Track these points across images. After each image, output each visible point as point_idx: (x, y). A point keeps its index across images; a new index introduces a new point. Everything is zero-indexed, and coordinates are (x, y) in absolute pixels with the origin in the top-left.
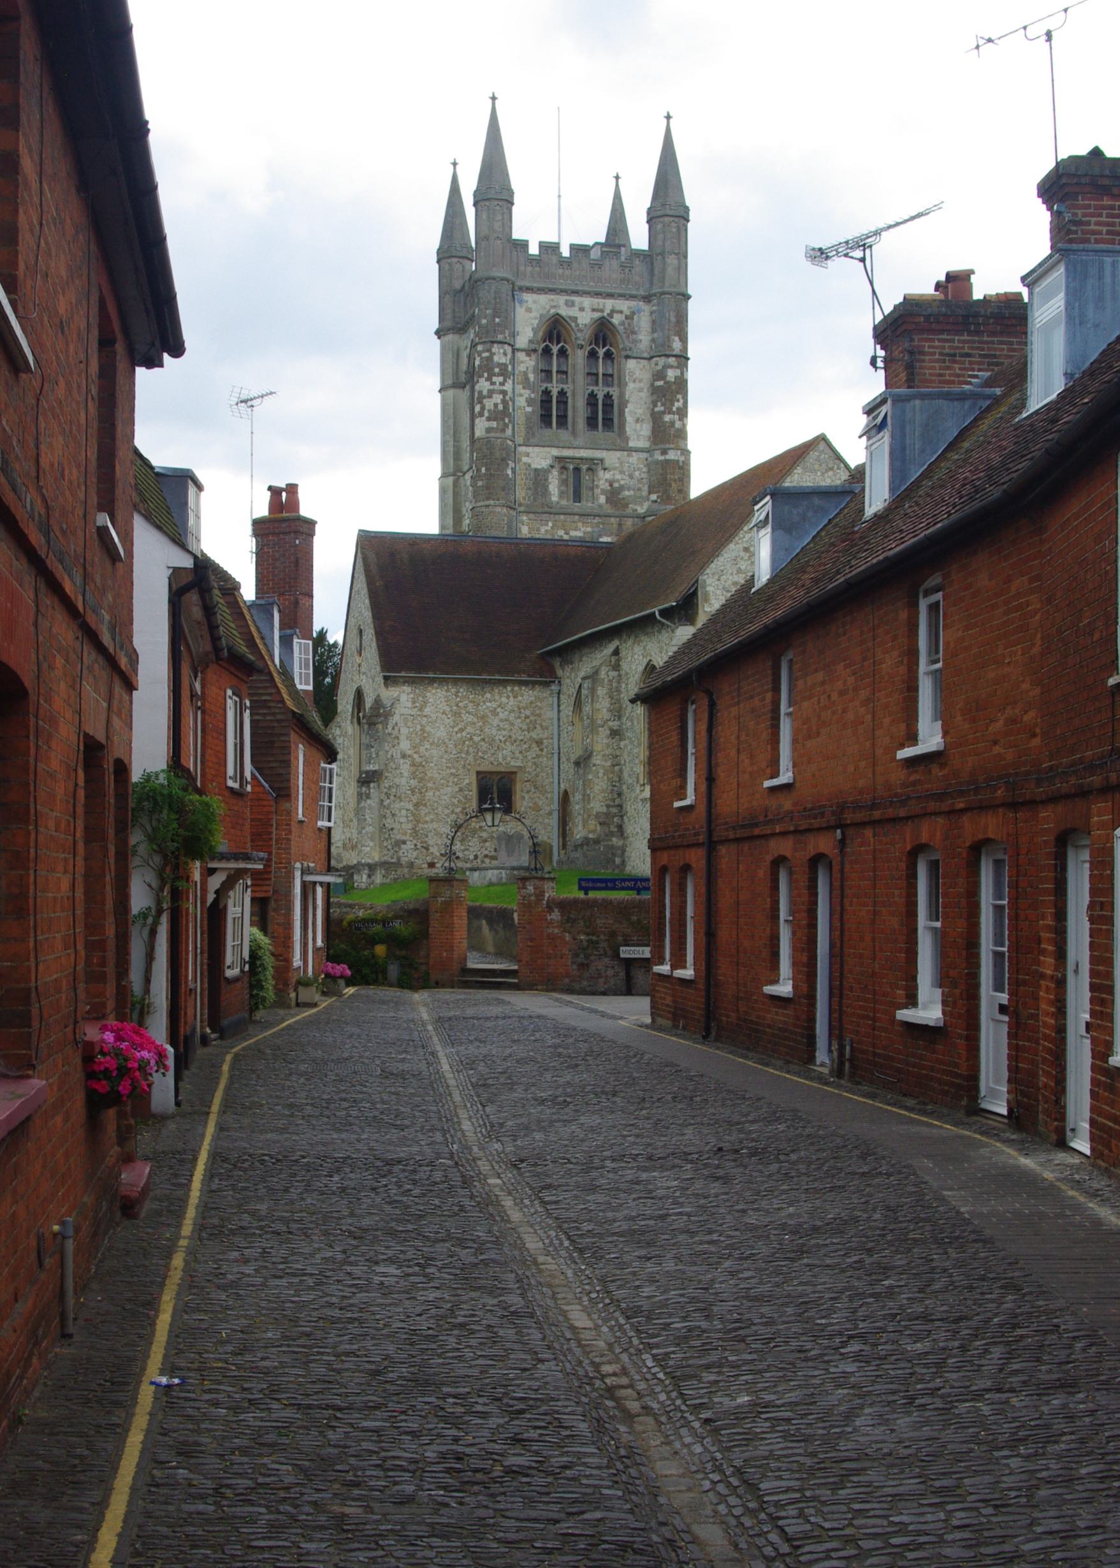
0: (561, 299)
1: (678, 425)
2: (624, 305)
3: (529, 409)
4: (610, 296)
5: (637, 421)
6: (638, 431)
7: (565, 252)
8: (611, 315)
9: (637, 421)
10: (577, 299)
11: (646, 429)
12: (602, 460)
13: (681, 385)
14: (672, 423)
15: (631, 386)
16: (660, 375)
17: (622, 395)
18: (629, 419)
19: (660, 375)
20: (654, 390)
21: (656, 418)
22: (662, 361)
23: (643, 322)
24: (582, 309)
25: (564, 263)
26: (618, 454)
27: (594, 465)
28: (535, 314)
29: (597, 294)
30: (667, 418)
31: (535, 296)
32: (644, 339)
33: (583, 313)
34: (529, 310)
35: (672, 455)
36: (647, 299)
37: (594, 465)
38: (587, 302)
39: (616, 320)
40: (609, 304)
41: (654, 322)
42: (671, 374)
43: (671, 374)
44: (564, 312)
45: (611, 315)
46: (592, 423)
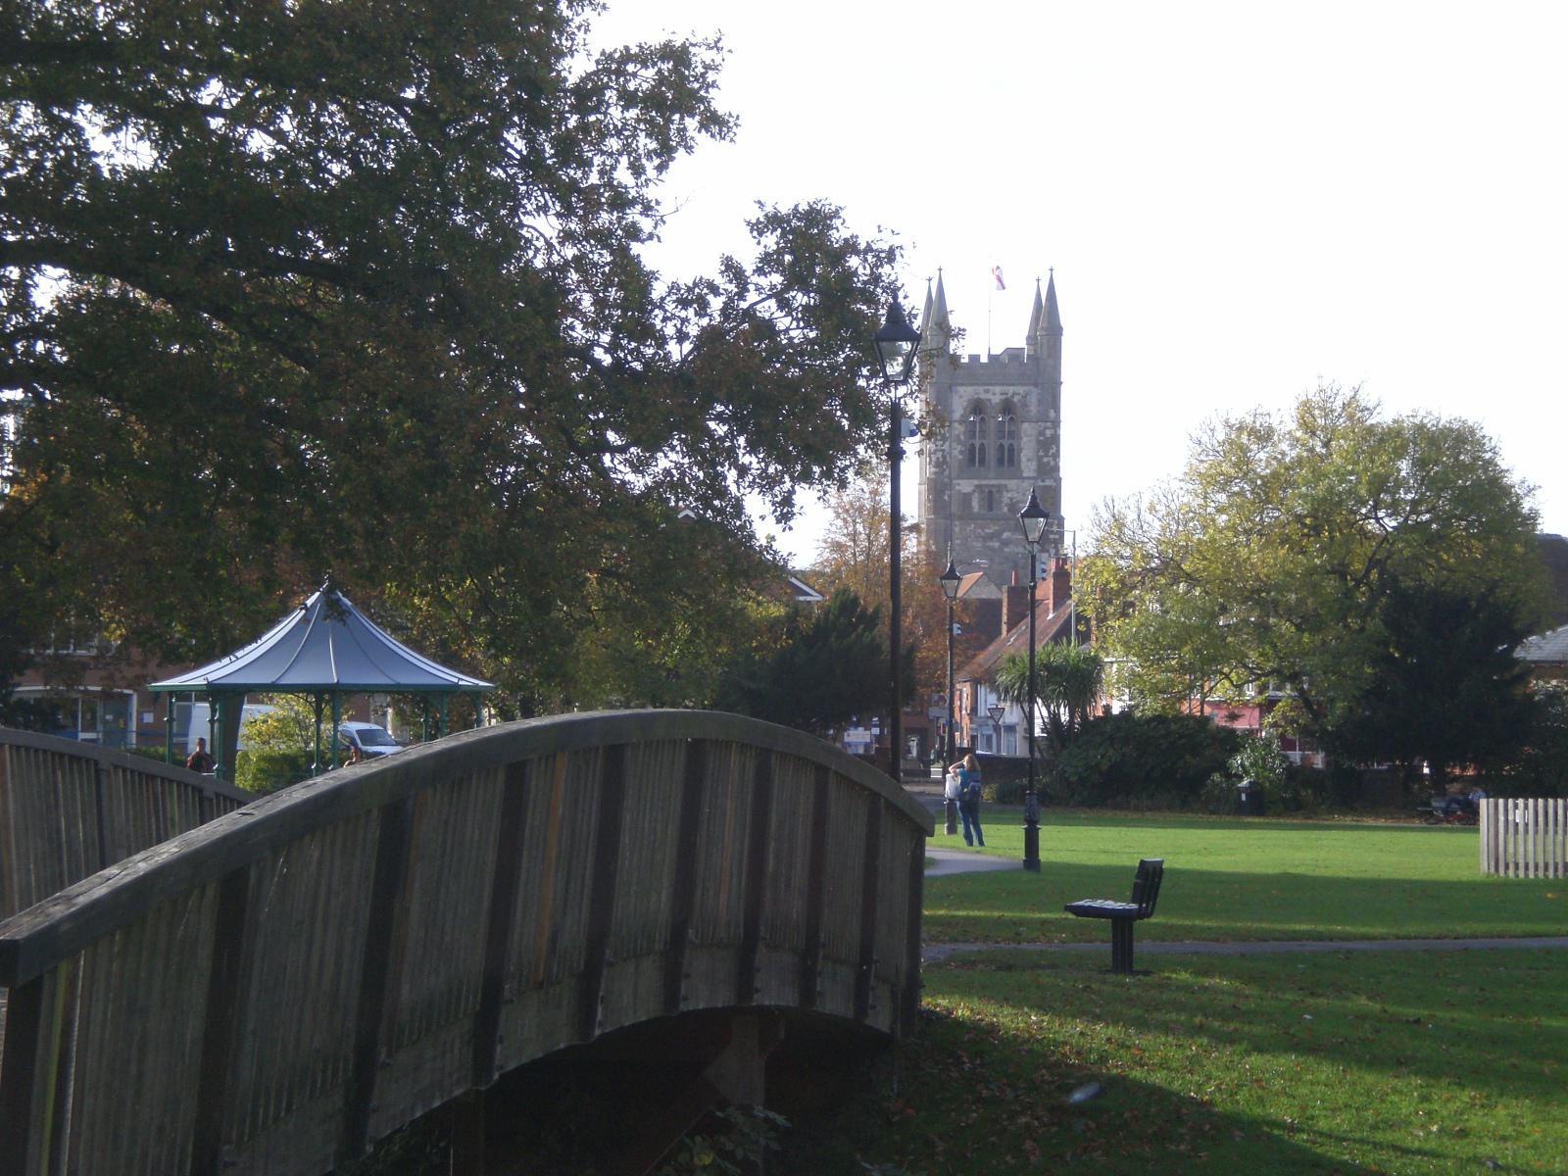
0: (981, 389)
1: (1052, 463)
2: (1021, 390)
3: (960, 457)
4: (1013, 385)
5: (1029, 460)
6: (1028, 466)
7: (984, 359)
8: (1012, 397)
9: (1029, 460)
11: (1034, 465)
12: (1005, 486)
13: (1055, 440)
14: (1048, 463)
15: (1025, 439)
16: (1042, 433)
17: (1019, 445)
18: (1023, 459)
19: (1042, 433)
20: (1039, 442)
21: (1039, 459)
22: (1043, 424)
23: (1033, 400)
24: (994, 394)
26: (1015, 481)
27: (1001, 489)
29: (1003, 385)
30: (1045, 460)
32: (1033, 409)
33: (995, 395)
34: (961, 397)
35: (1048, 483)
36: (1036, 385)
37: (1001, 489)
38: (998, 389)
39: (1016, 399)
40: (1011, 390)
41: (1039, 400)
42: (1048, 433)
43: (1048, 433)
44: (983, 396)
45: (1012, 397)
46: (1001, 461)
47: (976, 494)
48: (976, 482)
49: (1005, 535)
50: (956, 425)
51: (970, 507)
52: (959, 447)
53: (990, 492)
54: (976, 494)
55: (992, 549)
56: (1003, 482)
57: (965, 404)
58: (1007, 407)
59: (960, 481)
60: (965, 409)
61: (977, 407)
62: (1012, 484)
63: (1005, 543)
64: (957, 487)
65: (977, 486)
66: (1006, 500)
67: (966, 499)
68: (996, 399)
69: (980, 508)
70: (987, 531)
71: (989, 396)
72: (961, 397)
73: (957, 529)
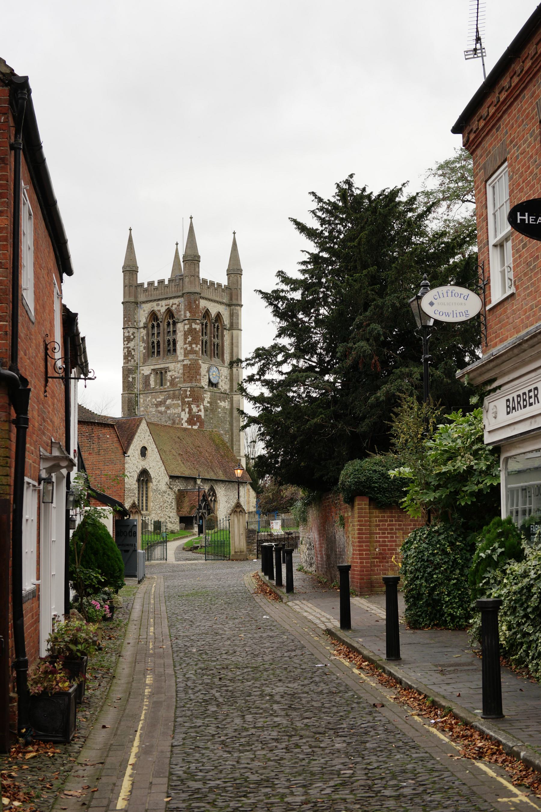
0: (155, 304)
2: (176, 301)
4: (171, 298)
8: (172, 306)
10: (160, 302)
12: (168, 367)
24: (162, 306)
25: (156, 289)
27: (166, 370)
28: (146, 312)
29: (166, 299)
31: (146, 305)
33: (161, 308)
37: (166, 370)
40: (171, 302)
44: (156, 308)
47: (152, 376)
48: (152, 367)
49: (169, 402)
50: (142, 330)
51: (149, 385)
52: (143, 345)
53: (161, 373)
54: (152, 376)
55: (161, 413)
56: (167, 365)
57: (146, 315)
58: (169, 313)
59: (143, 368)
60: (147, 319)
61: (153, 316)
62: (171, 366)
63: (168, 408)
64: (142, 372)
65: (153, 370)
66: (169, 378)
67: (147, 379)
68: (163, 310)
69: (156, 385)
70: (158, 400)
71: (159, 308)
72: (144, 311)
73: (142, 401)
